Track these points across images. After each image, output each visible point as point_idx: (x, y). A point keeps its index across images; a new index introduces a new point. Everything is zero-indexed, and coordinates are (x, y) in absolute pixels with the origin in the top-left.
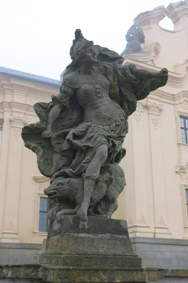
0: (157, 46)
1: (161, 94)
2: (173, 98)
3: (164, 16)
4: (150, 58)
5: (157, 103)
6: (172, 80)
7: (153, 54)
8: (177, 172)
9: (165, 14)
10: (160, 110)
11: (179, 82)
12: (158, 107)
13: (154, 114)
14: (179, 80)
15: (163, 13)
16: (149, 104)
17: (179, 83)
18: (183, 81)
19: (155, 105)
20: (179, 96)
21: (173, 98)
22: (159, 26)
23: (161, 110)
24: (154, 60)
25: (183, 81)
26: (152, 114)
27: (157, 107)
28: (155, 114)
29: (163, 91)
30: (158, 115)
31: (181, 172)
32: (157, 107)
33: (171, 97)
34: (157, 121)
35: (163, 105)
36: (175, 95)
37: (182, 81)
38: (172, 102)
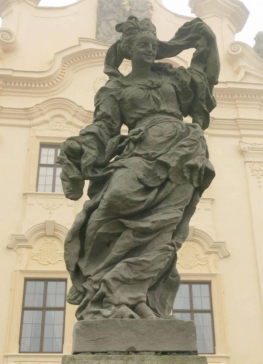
2: (27, 115)
17: (47, 88)
20: (40, 110)
21: (27, 115)
31: (20, 247)
36: (29, 109)
38: (27, 123)
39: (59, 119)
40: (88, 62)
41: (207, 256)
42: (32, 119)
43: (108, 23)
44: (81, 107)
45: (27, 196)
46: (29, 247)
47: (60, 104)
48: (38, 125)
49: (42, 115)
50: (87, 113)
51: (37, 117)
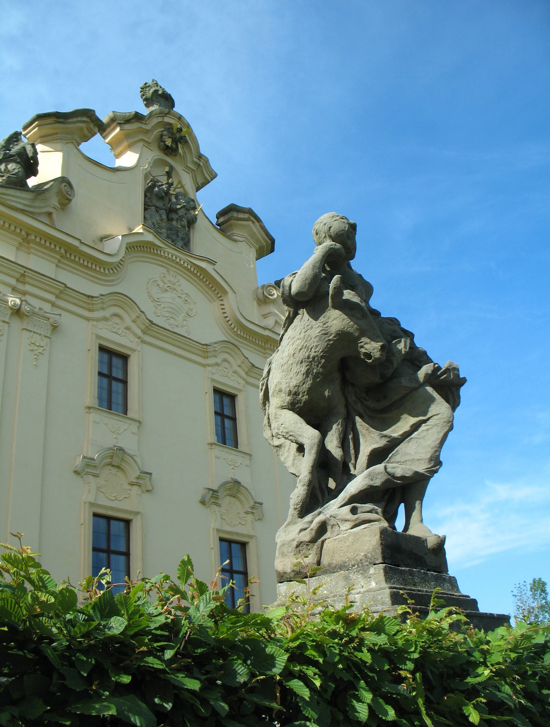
0: (65, 186)
1: (58, 289)
3: (94, 134)
4: (44, 207)
5: (47, 307)
6: (90, 265)
7: (54, 201)
8: (76, 472)
9: (96, 130)
10: (52, 325)
11: (107, 272)
12: (49, 319)
13: (37, 333)
14: (108, 269)
15: (92, 126)
16: (26, 308)
17: (106, 275)
18: (115, 271)
19: (40, 313)
20: (103, 303)
21: (88, 304)
22: (79, 150)
23: (55, 328)
24: (54, 216)
25: (115, 271)
26: (31, 331)
27: (45, 317)
28: (39, 332)
29: (65, 285)
30: (45, 336)
32: (45, 317)
33: (85, 302)
34: (42, 349)
35: (60, 315)
36: (93, 297)
37: (114, 272)
39: (116, 319)
40: (149, 256)
41: (245, 515)
42: (93, 311)
43: (157, 211)
44: (143, 312)
45: (91, 410)
46: (96, 476)
47: (122, 301)
48: (97, 320)
49: (103, 309)
50: (148, 322)
51: (97, 310)
